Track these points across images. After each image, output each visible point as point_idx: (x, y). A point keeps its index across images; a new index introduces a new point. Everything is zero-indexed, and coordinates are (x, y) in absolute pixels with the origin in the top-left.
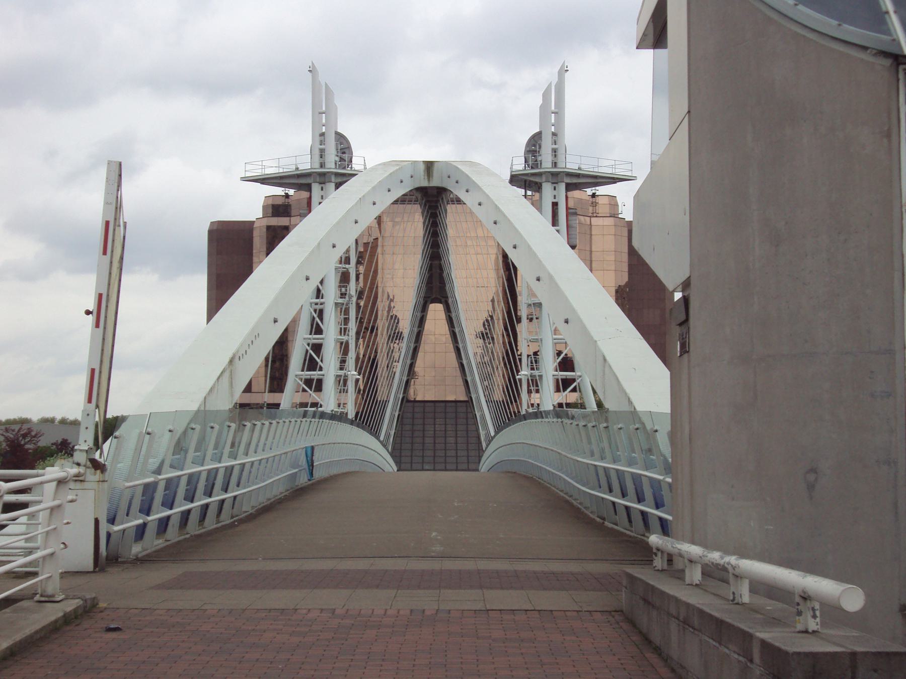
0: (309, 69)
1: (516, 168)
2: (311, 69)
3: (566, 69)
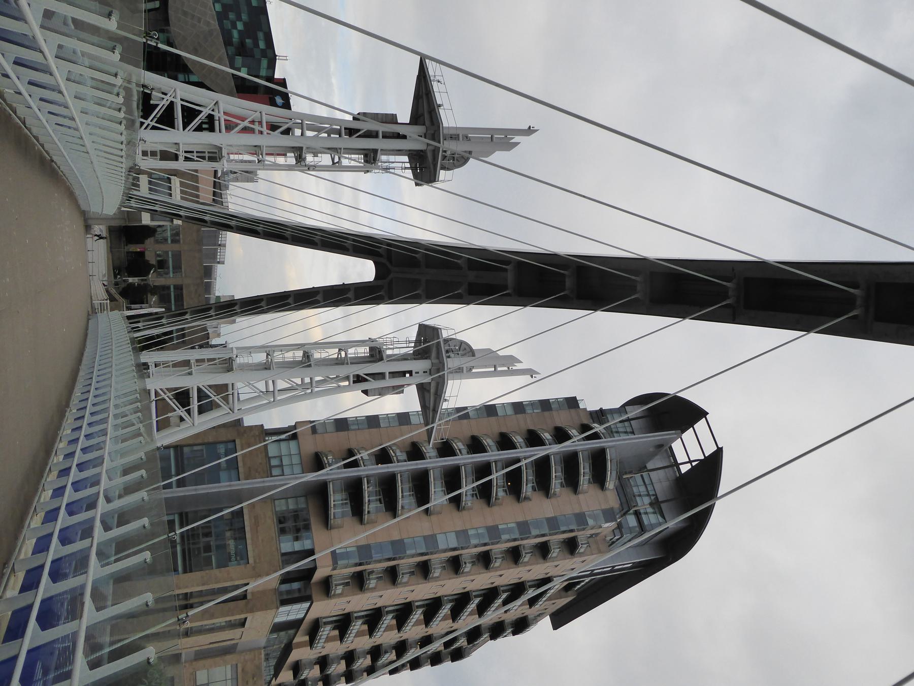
0: (531, 127)
2: (531, 128)
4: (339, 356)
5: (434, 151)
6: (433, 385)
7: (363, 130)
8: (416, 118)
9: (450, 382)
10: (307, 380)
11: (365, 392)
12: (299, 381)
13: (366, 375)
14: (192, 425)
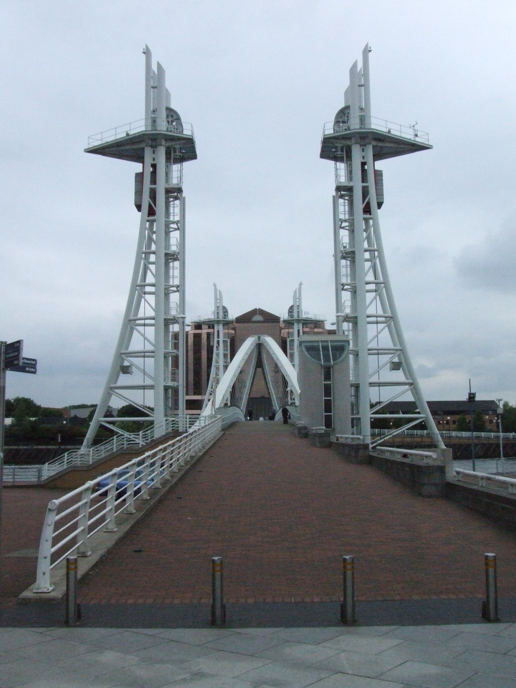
0: (143, 51)
1: (327, 132)
2: (145, 51)
3: (369, 49)
4: (347, 228)
5: (166, 140)
6: (375, 143)
7: (149, 203)
8: (139, 158)
9: (373, 127)
10: (367, 255)
11: (380, 205)
12: (368, 264)
13: (363, 202)
14: (401, 351)
